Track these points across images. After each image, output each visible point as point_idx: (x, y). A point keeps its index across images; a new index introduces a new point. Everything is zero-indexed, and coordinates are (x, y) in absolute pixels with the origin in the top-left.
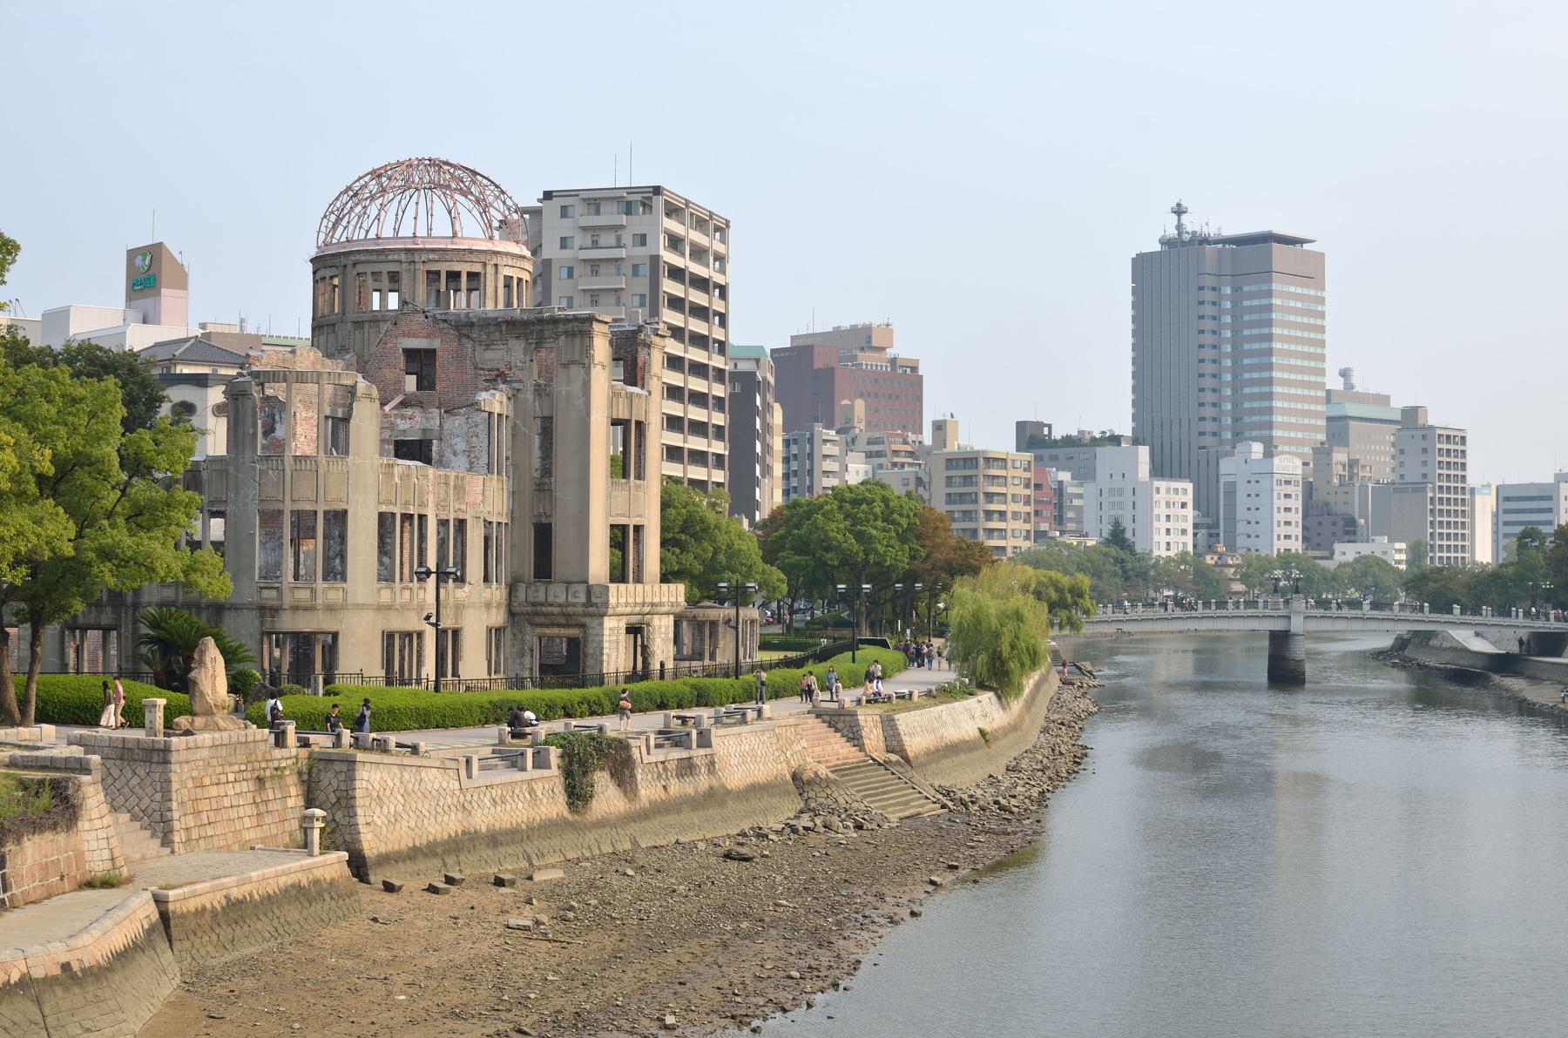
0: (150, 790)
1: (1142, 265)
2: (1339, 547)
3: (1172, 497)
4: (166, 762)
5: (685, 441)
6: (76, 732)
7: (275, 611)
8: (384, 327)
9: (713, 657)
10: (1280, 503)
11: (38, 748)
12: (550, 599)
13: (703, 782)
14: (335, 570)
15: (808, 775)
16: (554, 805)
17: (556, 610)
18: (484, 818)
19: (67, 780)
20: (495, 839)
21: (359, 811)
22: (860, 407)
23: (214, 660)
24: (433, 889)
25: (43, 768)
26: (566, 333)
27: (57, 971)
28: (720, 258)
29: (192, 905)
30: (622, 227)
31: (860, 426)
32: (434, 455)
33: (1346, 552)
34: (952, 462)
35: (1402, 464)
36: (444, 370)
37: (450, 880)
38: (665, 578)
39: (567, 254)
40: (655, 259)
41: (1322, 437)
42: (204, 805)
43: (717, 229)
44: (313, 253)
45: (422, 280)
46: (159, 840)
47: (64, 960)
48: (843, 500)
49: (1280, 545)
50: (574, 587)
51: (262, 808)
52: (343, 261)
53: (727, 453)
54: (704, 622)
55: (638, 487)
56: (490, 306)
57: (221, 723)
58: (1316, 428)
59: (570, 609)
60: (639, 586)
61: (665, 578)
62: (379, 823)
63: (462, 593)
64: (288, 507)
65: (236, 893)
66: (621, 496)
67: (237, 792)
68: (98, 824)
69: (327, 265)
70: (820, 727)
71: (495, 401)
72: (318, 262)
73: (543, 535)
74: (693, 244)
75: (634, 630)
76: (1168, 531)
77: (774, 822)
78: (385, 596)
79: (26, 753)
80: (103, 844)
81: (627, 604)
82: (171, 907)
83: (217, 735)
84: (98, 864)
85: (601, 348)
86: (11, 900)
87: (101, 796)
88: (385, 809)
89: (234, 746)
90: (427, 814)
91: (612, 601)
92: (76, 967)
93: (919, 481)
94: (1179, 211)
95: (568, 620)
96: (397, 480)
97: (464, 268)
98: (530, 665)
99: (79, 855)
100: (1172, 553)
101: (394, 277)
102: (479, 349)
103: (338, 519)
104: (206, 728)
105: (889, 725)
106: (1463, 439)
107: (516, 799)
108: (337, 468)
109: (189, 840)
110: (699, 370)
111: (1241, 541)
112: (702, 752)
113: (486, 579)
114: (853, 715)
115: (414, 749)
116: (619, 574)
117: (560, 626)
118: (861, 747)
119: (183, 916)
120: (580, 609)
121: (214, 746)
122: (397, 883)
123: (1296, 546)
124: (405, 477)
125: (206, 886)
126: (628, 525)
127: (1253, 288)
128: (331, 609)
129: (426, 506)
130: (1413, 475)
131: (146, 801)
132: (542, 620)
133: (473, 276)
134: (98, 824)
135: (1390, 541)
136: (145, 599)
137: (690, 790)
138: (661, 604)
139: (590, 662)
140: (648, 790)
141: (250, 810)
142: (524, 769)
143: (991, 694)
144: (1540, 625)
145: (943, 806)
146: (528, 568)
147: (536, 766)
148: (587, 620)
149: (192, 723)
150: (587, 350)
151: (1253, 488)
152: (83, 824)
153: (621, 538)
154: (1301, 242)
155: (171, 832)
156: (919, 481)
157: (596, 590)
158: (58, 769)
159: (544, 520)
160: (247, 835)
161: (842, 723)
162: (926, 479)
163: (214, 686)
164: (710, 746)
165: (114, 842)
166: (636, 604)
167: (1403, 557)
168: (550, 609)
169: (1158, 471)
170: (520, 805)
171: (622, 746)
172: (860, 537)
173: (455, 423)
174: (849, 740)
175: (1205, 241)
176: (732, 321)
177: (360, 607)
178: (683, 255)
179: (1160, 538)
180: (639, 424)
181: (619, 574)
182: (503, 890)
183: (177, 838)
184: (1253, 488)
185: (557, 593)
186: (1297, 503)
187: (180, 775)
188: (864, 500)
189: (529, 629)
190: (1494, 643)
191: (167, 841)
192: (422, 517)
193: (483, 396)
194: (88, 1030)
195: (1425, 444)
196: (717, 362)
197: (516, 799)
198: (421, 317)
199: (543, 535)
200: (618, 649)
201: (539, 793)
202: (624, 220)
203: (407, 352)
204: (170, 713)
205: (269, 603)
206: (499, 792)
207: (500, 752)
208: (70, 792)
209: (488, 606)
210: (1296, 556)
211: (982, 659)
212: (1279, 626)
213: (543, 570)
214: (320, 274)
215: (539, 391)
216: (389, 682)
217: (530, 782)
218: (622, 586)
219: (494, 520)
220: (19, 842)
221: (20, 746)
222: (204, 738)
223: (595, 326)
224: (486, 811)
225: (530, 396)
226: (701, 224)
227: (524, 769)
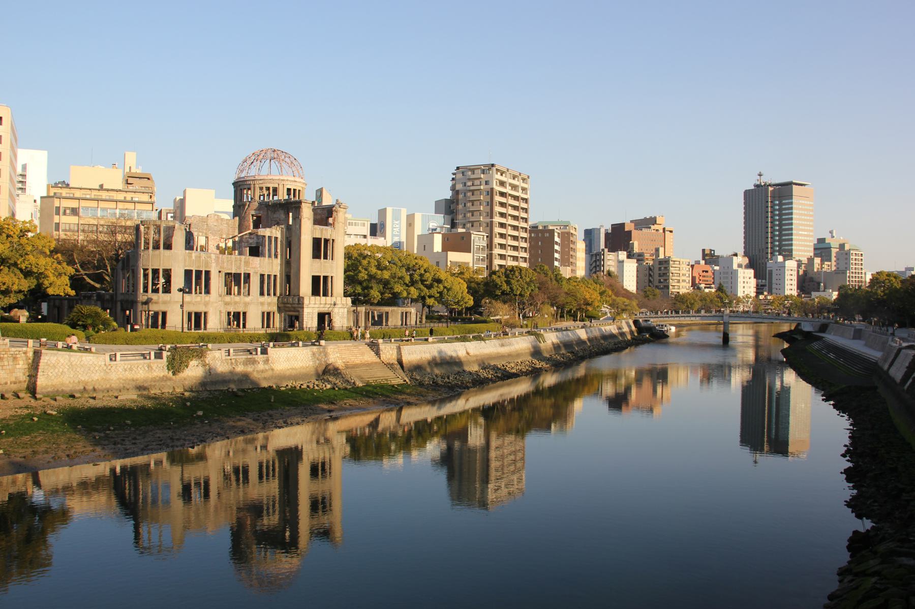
1: (747, 193)
5: (519, 254)
10: (787, 277)
14: (167, 290)
21: (40, 370)
28: (524, 189)
32: (260, 251)
35: (838, 264)
39: (465, 188)
40: (492, 189)
41: (812, 254)
45: (258, 191)
49: (787, 293)
53: (528, 257)
55: (325, 262)
58: (809, 251)
59: (294, 305)
60: (323, 298)
62: (51, 375)
63: (248, 299)
72: (235, 184)
74: (510, 184)
76: (744, 287)
81: (315, 304)
88: (57, 370)
90: (82, 373)
93: (650, 269)
94: (760, 175)
96: (194, 258)
97: (271, 186)
106: (862, 254)
107: (139, 369)
108: (167, 252)
110: (515, 228)
111: (774, 291)
112: (262, 356)
113: (262, 294)
118: (380, 359)
123: (795, 293)
126: (320, 276)
127: (787, 201)
128: (165, 303)
130: (842, 268)
132: (287, 309)
135: (832, 291)
145: (405, 381)
148: (299, 309)
151: (778, 272)
154: (804, 185)
156: (650, 269)
161: (374, 347)
162: (652, 268)
164: (267, 354)
166: (321, 304)
168: (288, 305)
170: (141, 372)
175: (770, 185)
176: (530, 211)
178: (506, 188)
180: (333, 240)
184: (778, 272)
192: (208, 273)
195: (846, 256)
196: (524, 225)
197: (139, 369)
200: (312, 320)
201: (154, 368)
202: (482, 176)
206: (129, 366)
209: (262, 304)
218: (313, 298)
224: (119, 373)
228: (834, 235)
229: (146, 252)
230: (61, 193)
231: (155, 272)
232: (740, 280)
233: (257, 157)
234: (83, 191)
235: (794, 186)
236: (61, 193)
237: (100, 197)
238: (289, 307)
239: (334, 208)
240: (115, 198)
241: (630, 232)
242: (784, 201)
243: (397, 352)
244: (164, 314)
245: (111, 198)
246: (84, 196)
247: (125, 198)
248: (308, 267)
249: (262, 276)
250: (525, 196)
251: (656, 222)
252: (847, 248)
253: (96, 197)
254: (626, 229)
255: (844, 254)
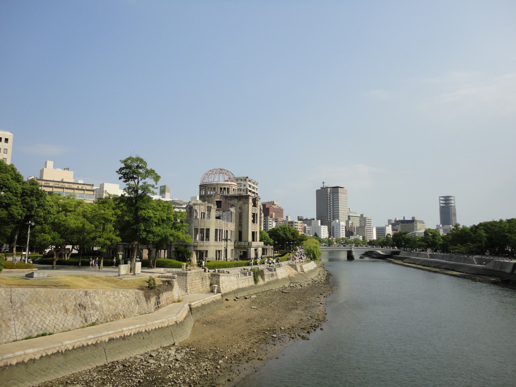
0: (183, 281)
1: (318, 192)
2: (351, 237)
3: (324, 229)
4: (186, 276)
6: (169, 270)
7: (197, 246)
8: (213, 197)
9: (266, 255)
10: (341, 229)
11: (163, 274)
12: (242, 244)
13: (275, 278)
15: (291, 276)
16: (252, 283)
17: (243, 246)
18: (241, 286)
19: (171, 280)
20: (243, 290)
21: (221, 285)
22: (274, 214)
23: (194, 256)
24: (235, 300)
25: (165, 278)
26: (245, 198)
27: (174, 323)
28: (257, 189)
29: (195, 306)
30: (241, 183)
31: (274, 217)
33: (352, 238)
34: (289, 223)
36: (223, 204)
37: (237, 298)
38: (260, 241)
40: (247, 189)
42: (193, 284)
43: (256, 184)
44: (200, 184)
46: (185, 292)
47: (176, 320)
48: (281, 228)
49: (341, 236)
50: (246, 242)
51: (203, 284)
52: (205, 185)
54: (265, 249)
56: (231, 193)
57: (196, 268)
61: (260, 241)
64: (199, 228)
65: (203, 303)
66: (254, 226)
67: (198, 281)
68: (176, 289)
69: (202, 187)
70: (290, 267)
71: (233, 210)
72: (201, 186)
73: (240, 234)
74: (253, 186)
75: (256, 250)
77: (287, 285)
78: (216, 244)
79: (162, 275)
80: (177, 293)
82: (192, 306)
83: (195, 270)
84: (176, 298)
85: (251, 201)
86: (161, 306)
87: (177, 283)
89: (198, 272)
91: (253, 245)
92: (178, 322)
94: (323, 183)
95: (245, 248)
97: (226, 187)
98: (238, 257)
99: (173, 296)
100: (324, 238)
101: (214, 188)
102: (229, 201)
103: (208, 230)
104: (193, 269)
105: (301, 266)
108: (208, 220)
109: (190, 291)
111: (335, 236)
112: (275, 272)
114: (296, 265)
115: (229, 273)
116: (253, 240)
117: (243, 249)
118: (297, 271)
119: (194, 308)
120: (247, 246)
121: (195, 273)
122: (228, 299)
123: (344, 236)
124: (220, 222)
125: (197, 302)
128: (207, 246)
129: (222, 227)
130: (363, 225)
131: (182, 284)
132: (240, 248)
133: (228, 188)
134: (176, 289)
136: (172, 244)
137: (273, 280)
138: (260, 245)
139: (248, 256)
140: (267, 280)
141: (201, 285)
142: (247, 276)
143: (313, 261)
144: (394, 250)
145: (312, 282)
146: (238, 239)
147: (249, 275)
148: (248, 248)
149: (190, 268)
150: (248, 201)
151: (337, 227)
152: (174, 289)
153: (253, 233)
154: (343, 188)
155: (187, 290)
157: (249, 243)
158: (168, 278)
159: (240, 231)
160: (201, 290)
161: (294, 266)
163: (194, 261)
165: (179, 293)
167: (362, 238)
169: (322, 224)
171: (262, 271)
172: (285, 234)
173: (225, 214)
174: (295, 270)
175: (328, 188)
177: (212, 246)
179: (322, 235)
180: (256, 214)
181: (253, 240)
182: (247, 300)
183: (188, 291)
184: (337, 227)
185: (243, 243)
186: (344, 230)
187: (189, 278)
188: (285, 228)
189: (237, 250)
190: (385, 253)
191: (186, 291)
193: (230, 209)
194: (181, 336)
198: (219, 195)
199: (240, 234)
203: (216, 201)
204: (187, 266)
205: (196, 245)
207: (242, 273)
208: (172, 283)
209: (231, 246)
210: (344, 238)
211: (312, 255)
212: (349, 250)
213: (240, 239)
214: (201, 188)
215: (240, 208)
216: (216, 259)
217: (248, 278)
219: (232, 230)
220: (162, 294)
221: (161, 273)
222: (193, 271)
223: (250, 197)
225: (238, 209)
226: (254, 183)
227: (247, 276)
228: (351, 210)
229: (203, 220)
230: (42, 183)
231: (202, 230)
232: (322, 231)
233: (213, 172)
234: (54, 183)
235: (339, 188)
236: (42, 183)
237: (64, 186)
238: (242, 247)
239: (257, 199)
240: (72, 187)
241: (269, 208)
242: (334, 195)
243: (301, 268)
244: (207, 251)
245: (70, 187)
246: (55, 185)
247: (78, 187)
248: (252, 228)
249: (231, 231)
250: (257, 192)
251: (274, 203)
252: (364, 216)
253: (62, 186)
254: (267, 207)
255: (363, 219)
